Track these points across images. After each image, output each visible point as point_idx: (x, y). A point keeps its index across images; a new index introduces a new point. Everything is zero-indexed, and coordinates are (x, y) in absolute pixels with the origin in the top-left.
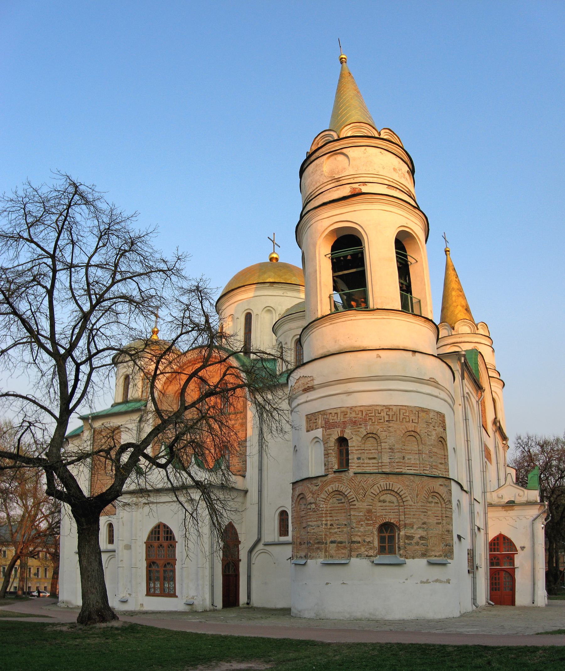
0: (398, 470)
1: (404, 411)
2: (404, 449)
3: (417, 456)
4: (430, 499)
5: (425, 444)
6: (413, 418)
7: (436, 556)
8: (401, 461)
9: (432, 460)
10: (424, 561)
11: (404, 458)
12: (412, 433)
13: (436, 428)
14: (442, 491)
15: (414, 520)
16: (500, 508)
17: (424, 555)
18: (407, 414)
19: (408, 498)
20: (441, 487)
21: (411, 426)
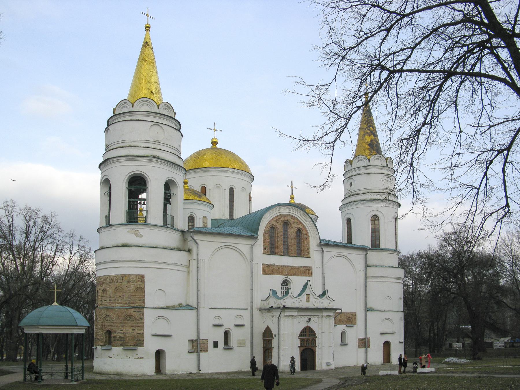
0: (112, 306)
1: (115, 277)
2: (116, 296)
3: (122, 299)
4: (128, 319)
5: (125, 292)
6: (120, 280)
7: (131, 345)
8: (115, 301)
9: (130, 300)
10: (121, 348)
11: (115, 300)
12: (120, 288)
13: (135, 283)
14: (136, 314)
15: (117, 329)
16: (266, 311)
17: (121, 345)
18: (117, 279)
19: (114, 319)
20: (135, 313)
21: (118, 284)
